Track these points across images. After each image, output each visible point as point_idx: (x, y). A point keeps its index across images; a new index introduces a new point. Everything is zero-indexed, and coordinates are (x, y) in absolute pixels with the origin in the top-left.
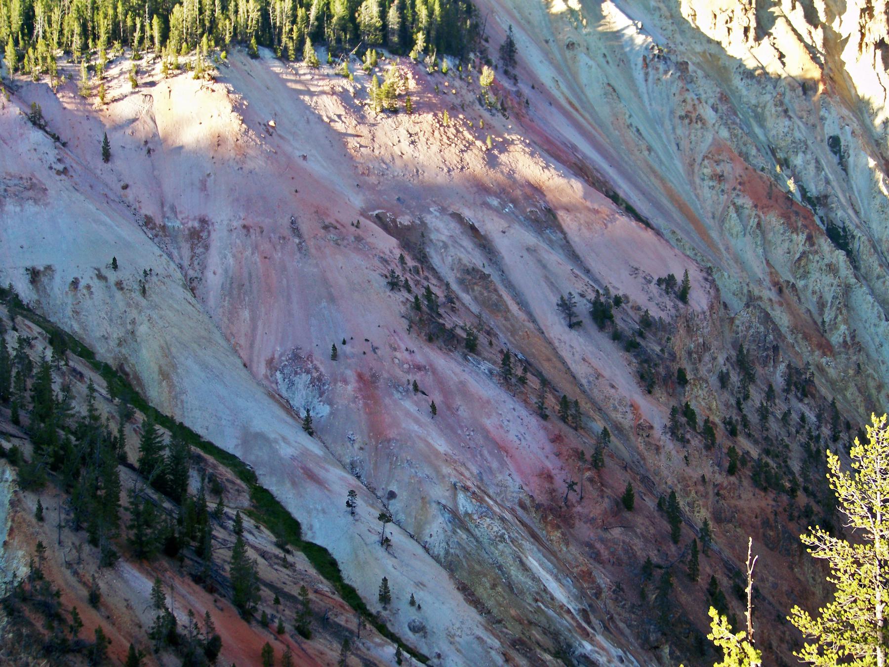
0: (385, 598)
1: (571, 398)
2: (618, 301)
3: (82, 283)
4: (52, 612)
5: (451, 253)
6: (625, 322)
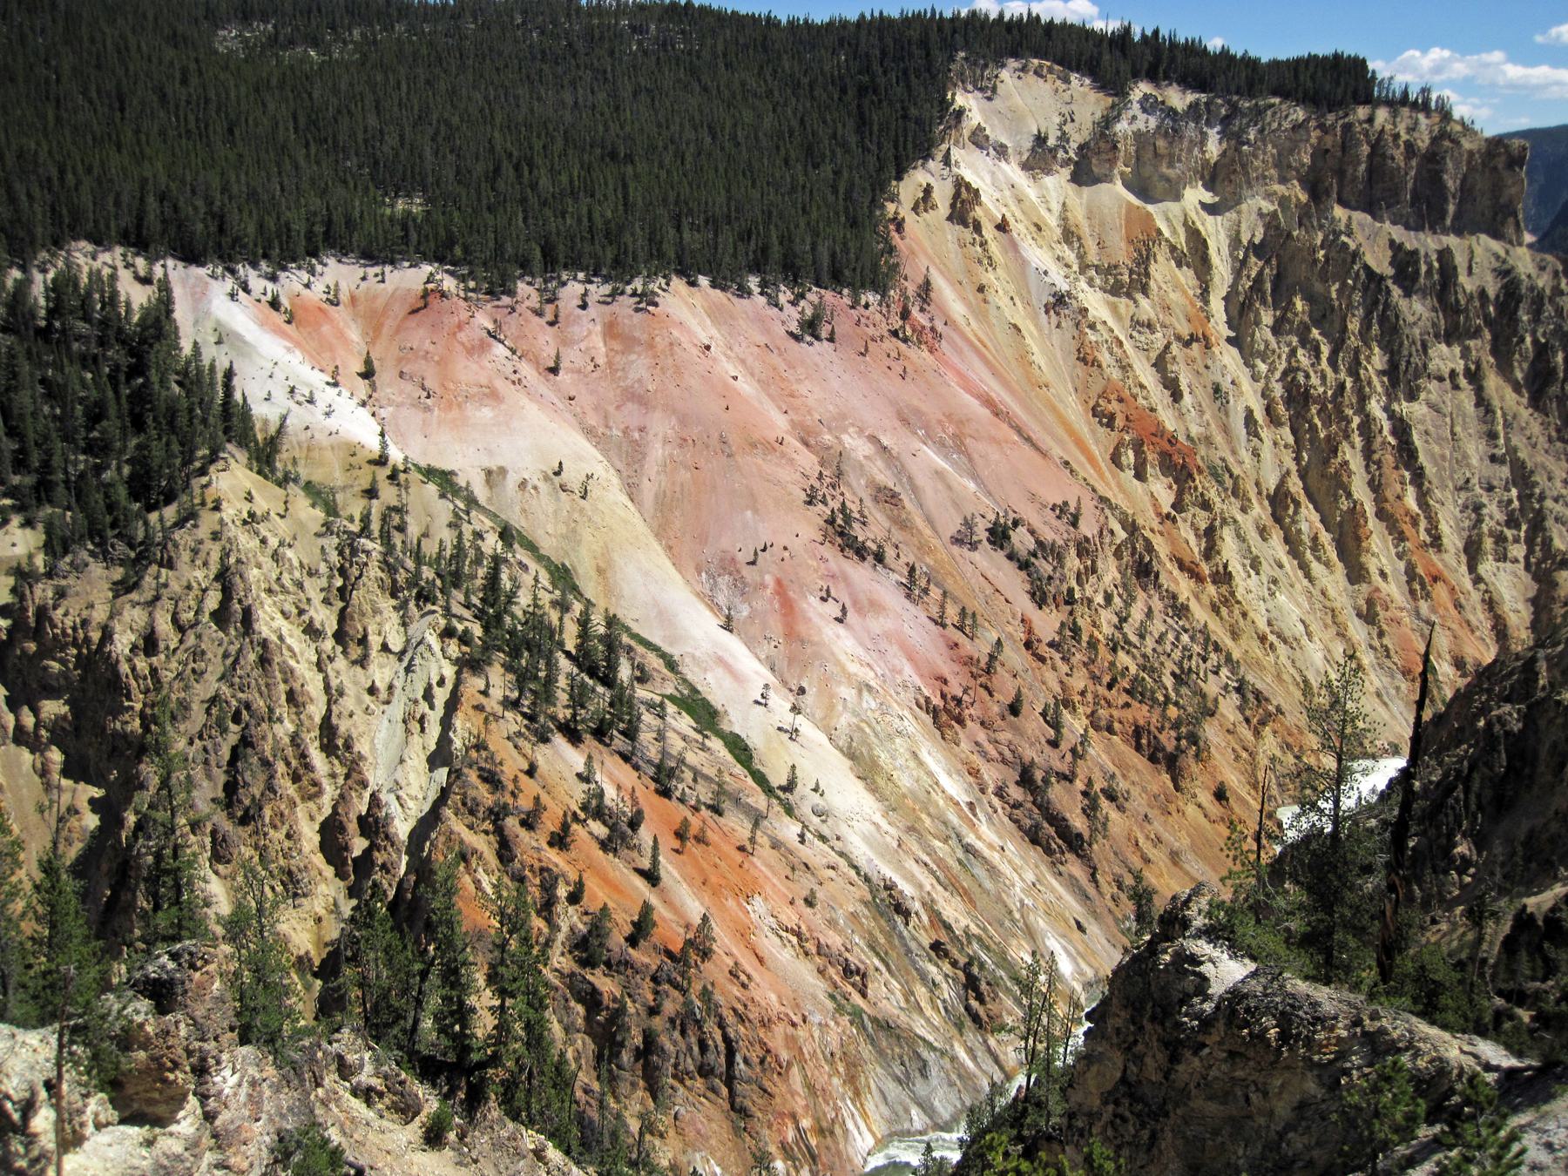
3: (529, 487)
4: (491, 779)
6: (1022, 540)
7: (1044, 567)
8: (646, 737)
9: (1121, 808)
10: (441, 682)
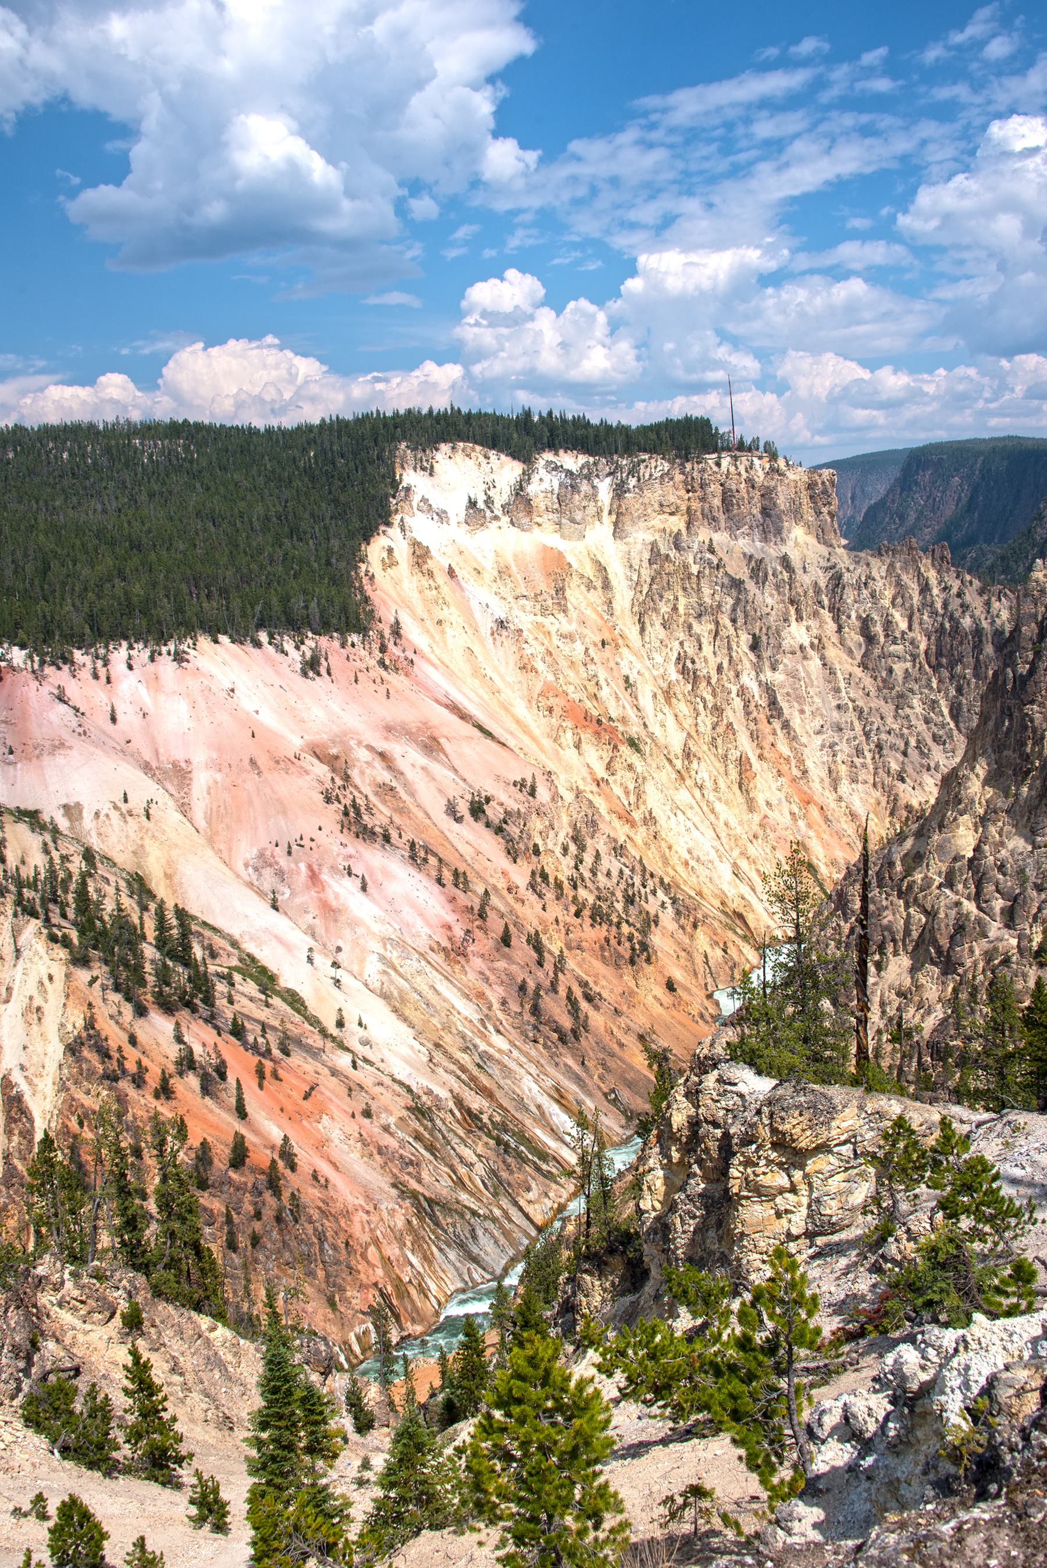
0: (340, 1024)
1: (461, 870)
2: (488, 800)
5: (367, 775)
6: (494, 812)
7: (514, 830)
8: (221, 1003)
9: (597, 1008)
10: (51, 978)
